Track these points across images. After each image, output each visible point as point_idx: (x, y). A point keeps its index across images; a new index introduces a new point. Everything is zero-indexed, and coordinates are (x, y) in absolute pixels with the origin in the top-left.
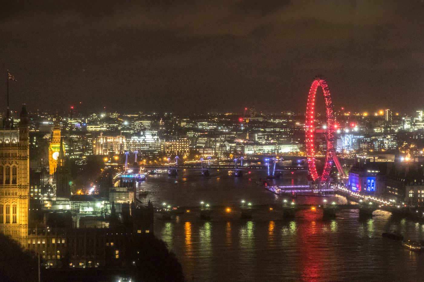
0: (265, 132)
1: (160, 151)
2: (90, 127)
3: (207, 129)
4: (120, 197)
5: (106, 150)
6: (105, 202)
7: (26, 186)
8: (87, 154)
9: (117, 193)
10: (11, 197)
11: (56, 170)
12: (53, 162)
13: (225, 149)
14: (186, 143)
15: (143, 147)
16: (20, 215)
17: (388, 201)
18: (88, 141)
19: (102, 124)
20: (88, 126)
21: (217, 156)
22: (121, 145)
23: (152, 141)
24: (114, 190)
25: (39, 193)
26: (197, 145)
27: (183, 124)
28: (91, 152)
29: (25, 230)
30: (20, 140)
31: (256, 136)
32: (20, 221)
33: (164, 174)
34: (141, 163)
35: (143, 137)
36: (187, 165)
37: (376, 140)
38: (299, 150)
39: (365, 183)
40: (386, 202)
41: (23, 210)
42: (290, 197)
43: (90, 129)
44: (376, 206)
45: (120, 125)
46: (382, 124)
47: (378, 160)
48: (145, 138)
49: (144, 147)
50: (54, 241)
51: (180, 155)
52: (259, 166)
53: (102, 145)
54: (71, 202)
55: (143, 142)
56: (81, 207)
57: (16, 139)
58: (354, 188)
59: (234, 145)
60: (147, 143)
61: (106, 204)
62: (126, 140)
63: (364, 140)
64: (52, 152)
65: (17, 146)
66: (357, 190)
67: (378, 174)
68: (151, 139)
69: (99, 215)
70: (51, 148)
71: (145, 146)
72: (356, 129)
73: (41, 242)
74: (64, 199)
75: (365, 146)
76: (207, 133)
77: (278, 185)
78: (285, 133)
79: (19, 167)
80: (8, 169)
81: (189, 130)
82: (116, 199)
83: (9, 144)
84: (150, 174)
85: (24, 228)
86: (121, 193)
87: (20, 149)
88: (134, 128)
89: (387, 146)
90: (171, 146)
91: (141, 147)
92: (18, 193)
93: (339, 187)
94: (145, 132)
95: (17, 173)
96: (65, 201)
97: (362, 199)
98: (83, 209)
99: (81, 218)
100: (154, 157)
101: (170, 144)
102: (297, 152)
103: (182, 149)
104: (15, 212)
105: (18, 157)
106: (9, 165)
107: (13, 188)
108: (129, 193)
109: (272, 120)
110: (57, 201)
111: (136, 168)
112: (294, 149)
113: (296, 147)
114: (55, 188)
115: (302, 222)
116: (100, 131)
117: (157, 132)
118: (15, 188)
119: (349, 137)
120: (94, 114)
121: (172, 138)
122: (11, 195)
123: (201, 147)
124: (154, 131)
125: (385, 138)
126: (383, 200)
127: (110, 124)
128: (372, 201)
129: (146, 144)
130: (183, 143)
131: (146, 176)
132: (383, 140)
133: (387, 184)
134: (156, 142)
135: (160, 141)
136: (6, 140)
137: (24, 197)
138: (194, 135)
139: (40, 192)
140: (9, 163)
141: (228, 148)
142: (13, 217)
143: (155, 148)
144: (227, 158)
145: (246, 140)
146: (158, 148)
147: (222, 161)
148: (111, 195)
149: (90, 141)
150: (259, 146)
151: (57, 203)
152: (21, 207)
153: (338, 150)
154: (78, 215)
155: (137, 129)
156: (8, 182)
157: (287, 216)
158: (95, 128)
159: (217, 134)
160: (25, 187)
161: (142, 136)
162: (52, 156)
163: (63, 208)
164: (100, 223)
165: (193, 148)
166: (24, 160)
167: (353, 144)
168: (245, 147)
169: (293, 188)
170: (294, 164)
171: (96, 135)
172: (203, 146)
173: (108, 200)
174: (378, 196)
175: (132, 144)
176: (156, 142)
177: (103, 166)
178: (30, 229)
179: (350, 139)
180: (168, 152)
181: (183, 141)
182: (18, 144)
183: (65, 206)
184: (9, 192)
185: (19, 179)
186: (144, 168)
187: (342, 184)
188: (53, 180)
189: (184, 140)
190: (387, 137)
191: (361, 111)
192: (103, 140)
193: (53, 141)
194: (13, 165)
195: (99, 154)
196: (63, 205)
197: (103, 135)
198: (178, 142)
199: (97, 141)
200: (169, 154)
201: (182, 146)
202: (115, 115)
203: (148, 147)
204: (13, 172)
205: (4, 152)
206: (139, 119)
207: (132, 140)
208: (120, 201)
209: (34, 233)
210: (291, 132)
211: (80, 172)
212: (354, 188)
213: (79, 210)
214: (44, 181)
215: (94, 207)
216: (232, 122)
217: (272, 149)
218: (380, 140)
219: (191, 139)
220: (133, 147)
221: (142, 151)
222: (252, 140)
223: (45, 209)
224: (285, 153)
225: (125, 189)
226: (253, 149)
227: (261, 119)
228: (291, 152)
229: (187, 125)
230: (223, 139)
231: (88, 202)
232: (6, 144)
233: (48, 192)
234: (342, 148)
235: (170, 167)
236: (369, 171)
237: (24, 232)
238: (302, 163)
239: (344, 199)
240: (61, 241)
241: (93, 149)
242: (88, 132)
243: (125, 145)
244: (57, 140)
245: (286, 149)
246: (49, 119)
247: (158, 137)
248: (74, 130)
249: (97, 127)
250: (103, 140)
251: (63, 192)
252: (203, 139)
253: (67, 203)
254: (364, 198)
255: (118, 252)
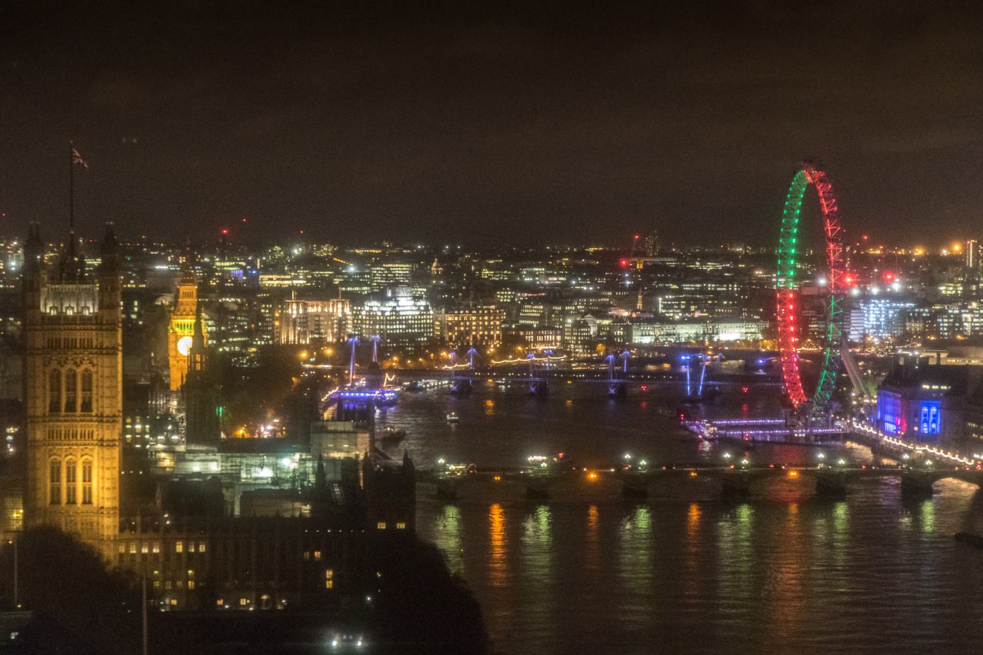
0: (680, 291)
1: (431, 335)
2: (266, 277)
3: (542, 285)
4: (338, 444)
5: (305, 333)
6: (301, 456)
7: (114, 416)
8: (259, 343)
9: (331, 436)
10: (79, 442)
11: (185, 380)
12: (178, 362)
13: (586, 332)
14: (495, 316)
15: (391, 327)
16: (100, 486)
17: (970, 458)
18: (263, 311)
19: (296, 272)
20: (261, 277)
21: (566, 348)
22: (340, 320)
23: (414, 313)
24: (323, 426)
25: (146, 433)
26: (521, 322)
27: (486, 273)
28: (269, 337)
29: (111, 519)
30: (99, 309)
31: (660, 302)
32: (100, 500)
33: (442, 392)
34: (387, 364)
35: (392, 304)
36: (496, 368)
37: (942, 312)
38: (760, 336)
39: (917, 414)
40: (965, 460)
41: (107, 474)
42: (740, 447)
43: (268, 283)
44: (946, 469)
45: (338, 273)
46: (958, 276)
47: (947, 360)
48: (398, 306)
49: (395, 327)
50: (179, 548)
51: (480, 346)
52: (667, 373)
53: (294, 321)
54: (222, 456)
55: (392, 315)
56: (243, 467)
57: (90, 305)
58: (890, 427)
59: (606, 322)
60: (401, 318)
61: (302, 461)
62: (352, 309)
63: (914, 313)
64: (177, 338)
65: (94, 322)
66: (897, 430)
67: (947, 393)
68: (410, 308)
69: (287, 486)
70: (174, 327)
71: (396, 324)
72: (896, 286)
73: (150, 550)
74: (204, 448)
75: (916, 326)
76: (543, 294)
77: (711, 417)
78: (729, 296)
79: (97, 372)
80: (72, 376)
81: (500, 285)
82: (328, 448)
83: (74, 318)
84: (407, 390)
85: (109, 517)
86: (338, 435)
87: (101, 329)
88: (372, 281)
89: (970, 328)
90: (458, 324)
91: (388, 327)
92: (95, 434)
93: (855, 424)
94: (397, 290)
95: (94, 388)
96: (207, 452)
97: (909, 452)
98: (248, 471)
99: (244, 492)
100: (419, 351)
101: (456, 319)
102: (756, 341)
103: (483, 330)
104: (87, 477)
105: (97, 348)
106: (74, 368)
107: (84, 421)
108: (359, 435)
109: (698, 264)
110: (189, 452)
111: (375, 374)
112: (750, 333)
113: (753, 328)
114: (183, 422)
115: (767, 509)
116: (291, 288)
117: (425, 290)
118: (88, 421)
119: (880, 305)
120: (277, 248)
121: (460, 304)
122: (79, 438)
123: (529, 327)
124: (419, 290)
125: (965, 307)
126: (957, 456)
127: (313, 271)
128: (932, 457)
129: (399, 320)
130: (486, 318)
131: (399, 394)
132: (961, 313)
133: (968, 418)
134: (423, 315)
135: (431, 312)
136: (67, 308)
137: (110, 444)
138: (514, 298)
139: (147, 431)
140: (75, 363)
141: (593, 330)
142: (84, 489)
143: (421, 328)
144: (591, 353)
145: (636, 311)
146: (427, 328)
147: (580, 361)
148: (315, 438)
149: (267, 311)
150: (667, 326)
151: (189, 456)
152: (103, 468)
153: (854, 336)
154: (237, 487)
155: (379, 284)
156: (71, 406)
157: (732, 491)
158: (278, 279)
159: (568, 297)
160: (112, 419)
161: (390, 299)
162: (176, 346)
163: (202, 470)
164: (289, 505)
165: (510, 329)
166: (111, 354)
167: (888, 321)
168: (634, 327)
169: (748, 427)
170: (749, 367)
171: (280, 296)
172: (535, 324)
173: (308, 451)
174: (946, 446)
175: (366, 320)
176: (423, 315)
177: (298, 370)
178: (123, 519)
179: (883, 309)
180: (451, 338)
181: (486, 312)
182: (96, 317)
183: (207, 465)
184: (75, 429)
185: (97, 401)
186: (394, 376)
187: (861, 418)
188: (178, 405)
189: (488, 310)
190: (969, 307)
191: (909, 244)
192: (298, 309)
193: (178, 310)
194: (83, 367)
195: (288, 341)
196: (202, 463)
197: (298, 297)
198: (474, 315)
199: (282, 312)
200: (453, 342)
201: (483, 325)
202: (326, 250)
203: (404, 326)
204: (83, 384)
205: (63, 336)
206: (383, 259)
207: (367, 308)
208: (336, 453)
209: (133, 528)
210: (741, 292)
211: (245, 384)
212: (890, 427)
213: (240, 473)
214: (156, 405)
215: (275, 467)
216: (604, 268)
217: (696, 334)
218: (953, 314)
219: (505, 308)
220: (367, 326)
221: (389, 336)
222: (650, 312)
223: (160, 472)
224: (728, 343)
225: (349, 426)
226: (651, 333)
227: (672, 262)
228: (741, 341)
229: (497, 274)
230: (582, 309)
231: (260, 456)
232: (66, 317)
233: (168, 431)
234: (861, 332)
235: (458, 373)
236: (926, 387)
237: (109, 525)
238: (768, 367)
239: (866, 452)
240: (197, 548)
241: (273, 329)
242: (260, 289)
243: (350, 322)
244: (188, 309)
245: (731, 333)
246: (169, 259)
247: (428, 303)
248: (229, 285)
249: (282, 277)
250: (298, 309)
251: (202, 431)
252: (535, 309)
253: (211, 457)
254: (915, 448)
255: (331, 573)
